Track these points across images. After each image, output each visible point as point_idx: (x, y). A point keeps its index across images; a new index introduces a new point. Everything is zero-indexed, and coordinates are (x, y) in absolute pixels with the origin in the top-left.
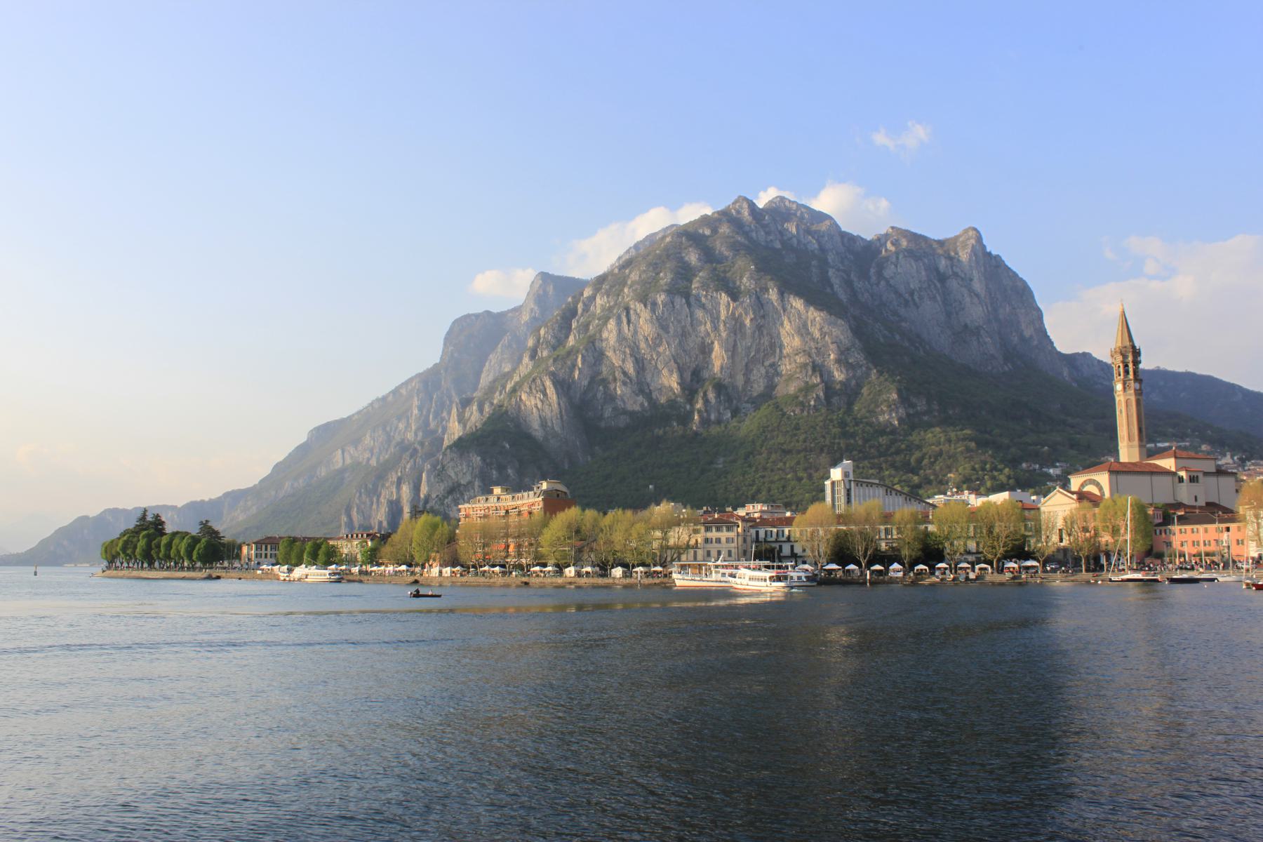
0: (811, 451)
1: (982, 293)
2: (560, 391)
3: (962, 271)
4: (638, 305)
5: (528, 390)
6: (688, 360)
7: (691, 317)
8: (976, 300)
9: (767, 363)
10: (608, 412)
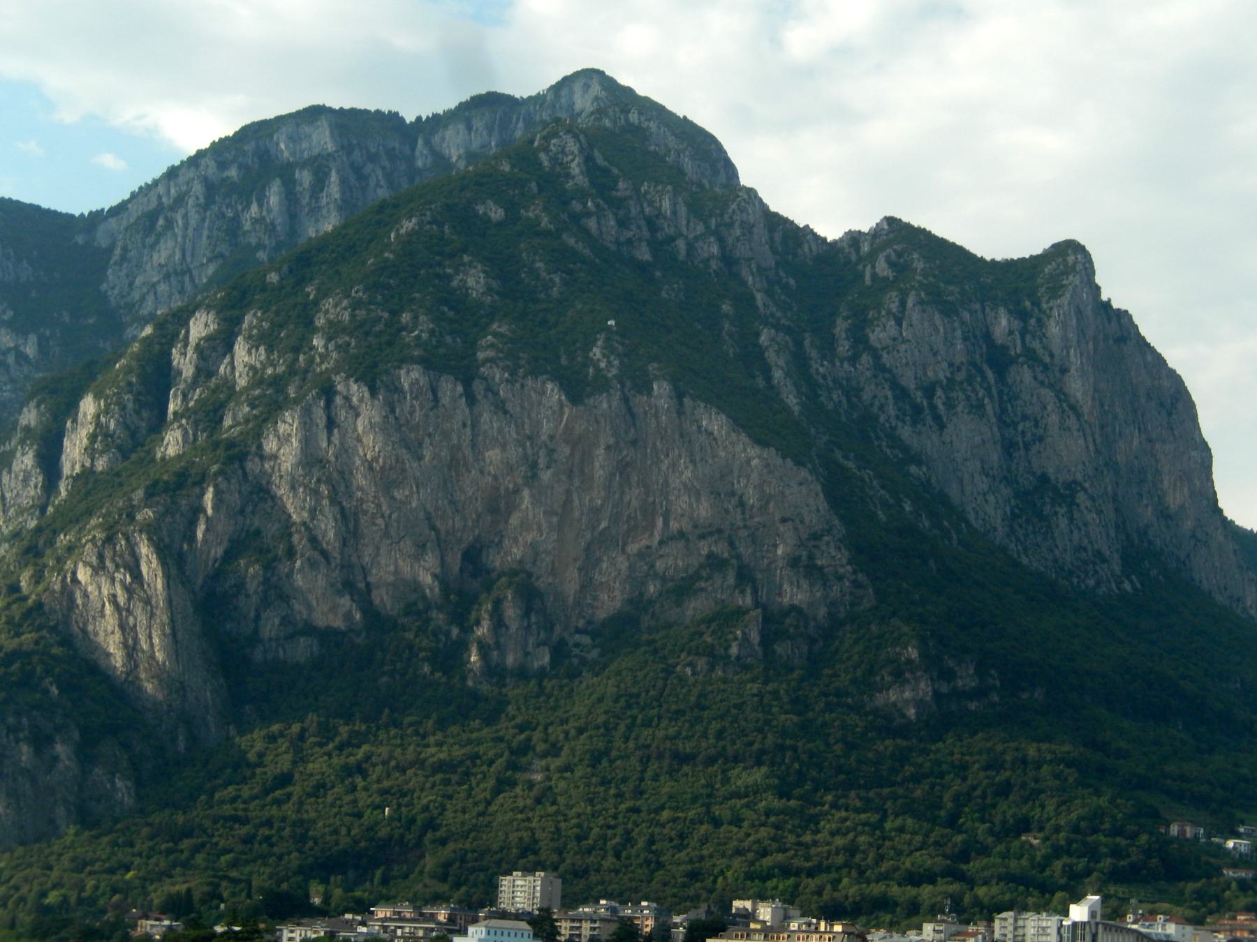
0: (736, 759)
1: (1086, 406)
2: (174, 572)
3: (1045, 348)
4: (354, 387)
5: (94, 560)
6: (459, 524)
7: (473, 426)
8: (1072, 422)
9: (633, 548)
10: (270, 626)
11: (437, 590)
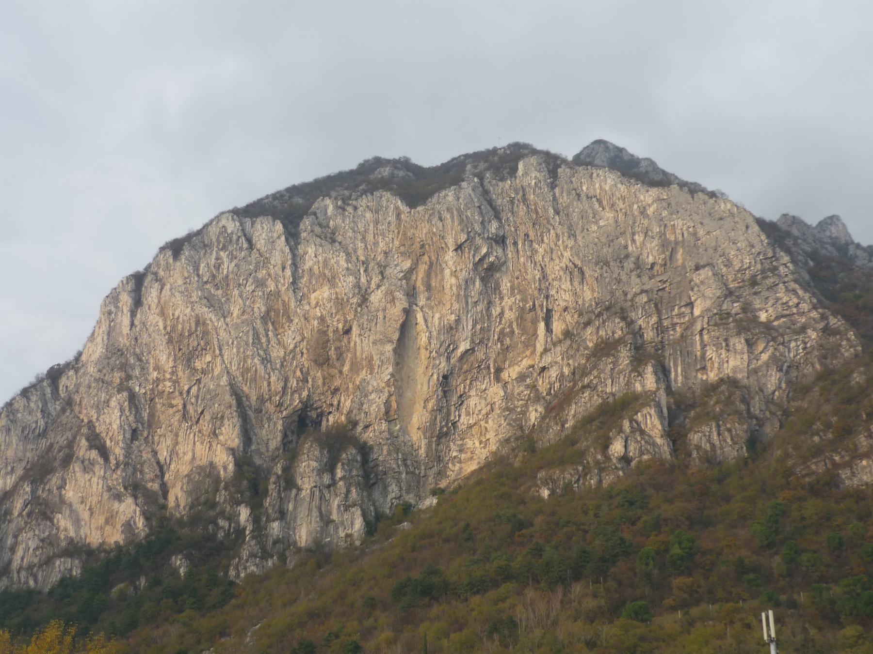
11: (231, 467)
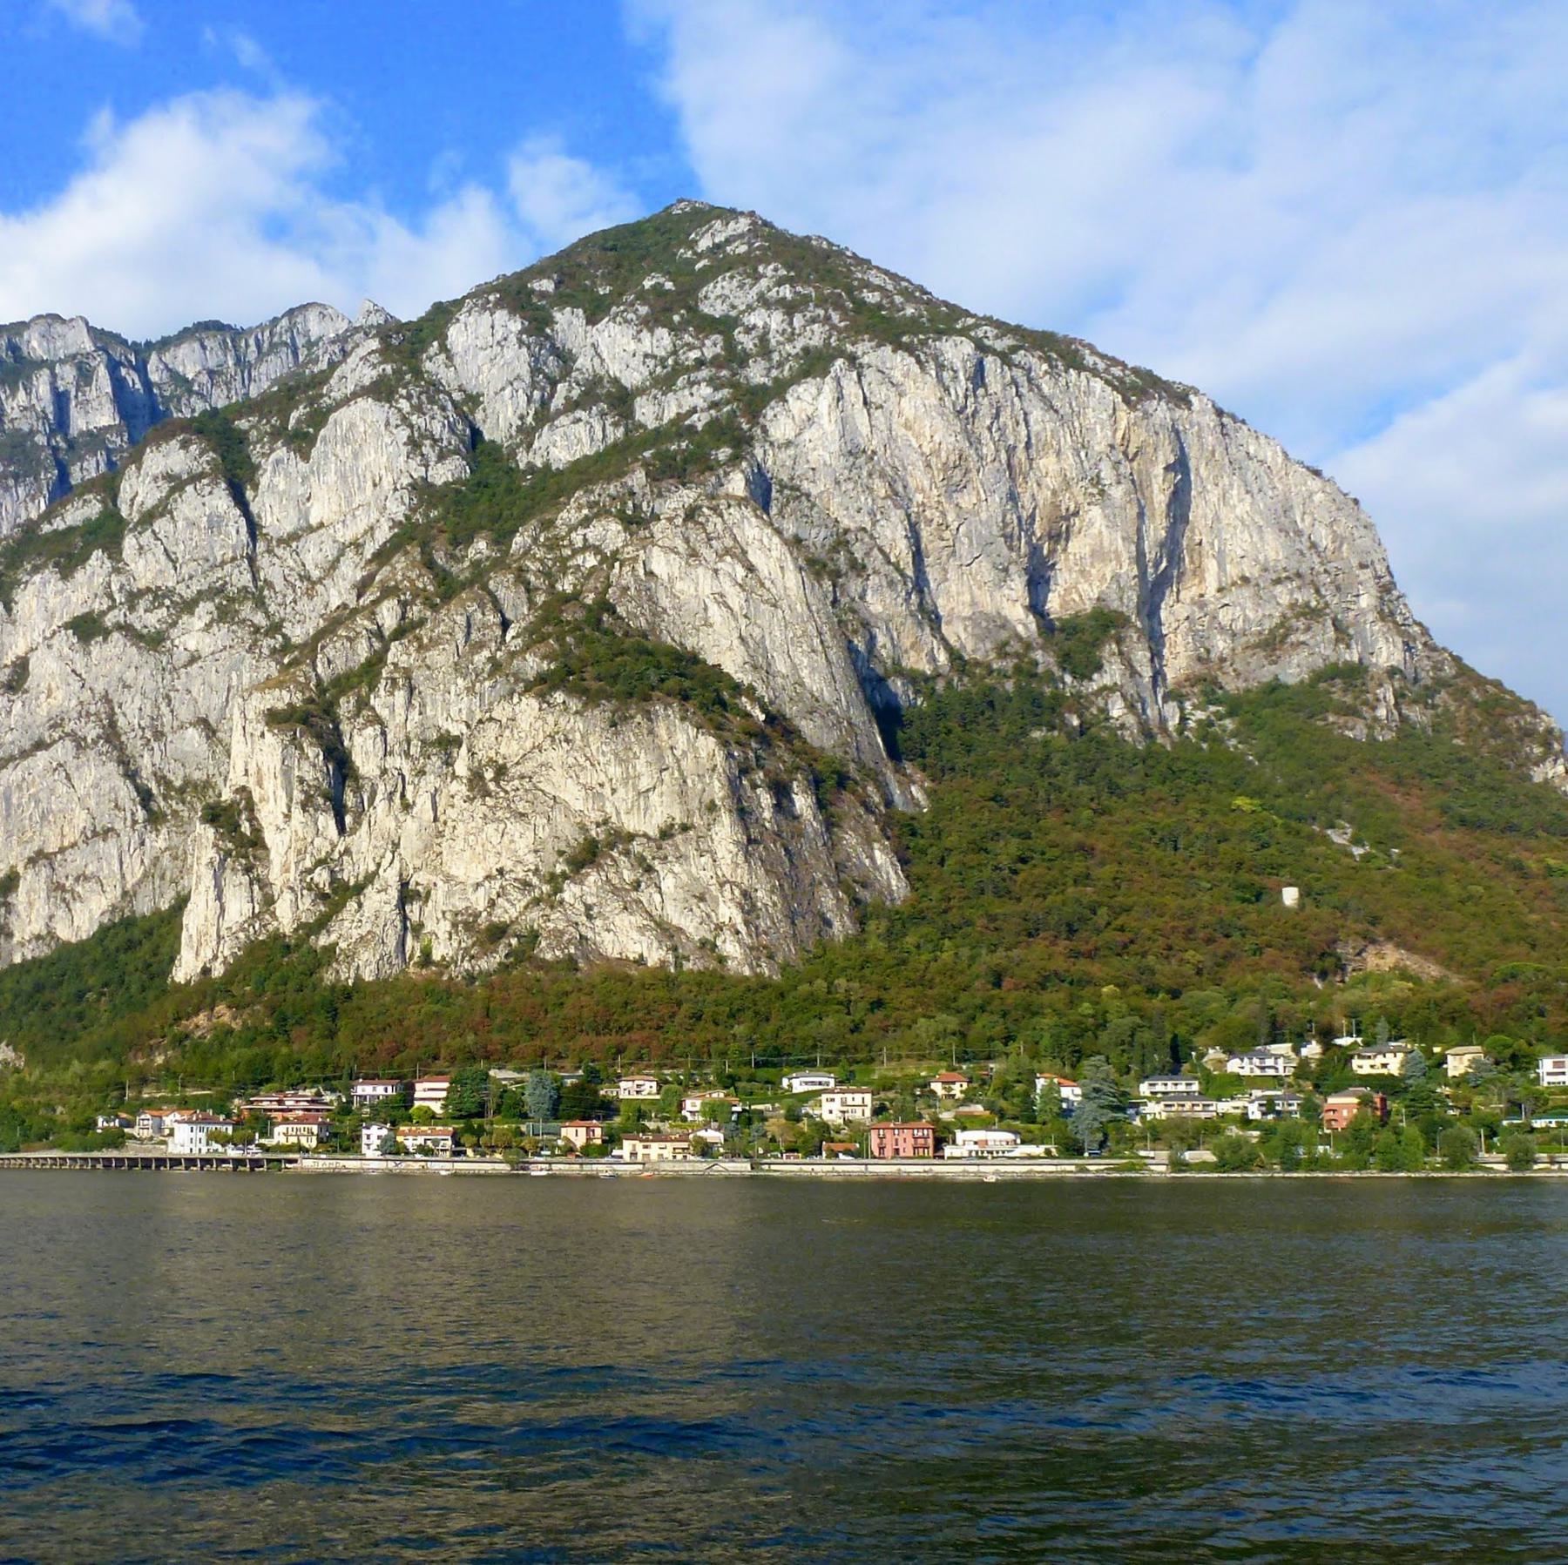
11: (1033, 627)
